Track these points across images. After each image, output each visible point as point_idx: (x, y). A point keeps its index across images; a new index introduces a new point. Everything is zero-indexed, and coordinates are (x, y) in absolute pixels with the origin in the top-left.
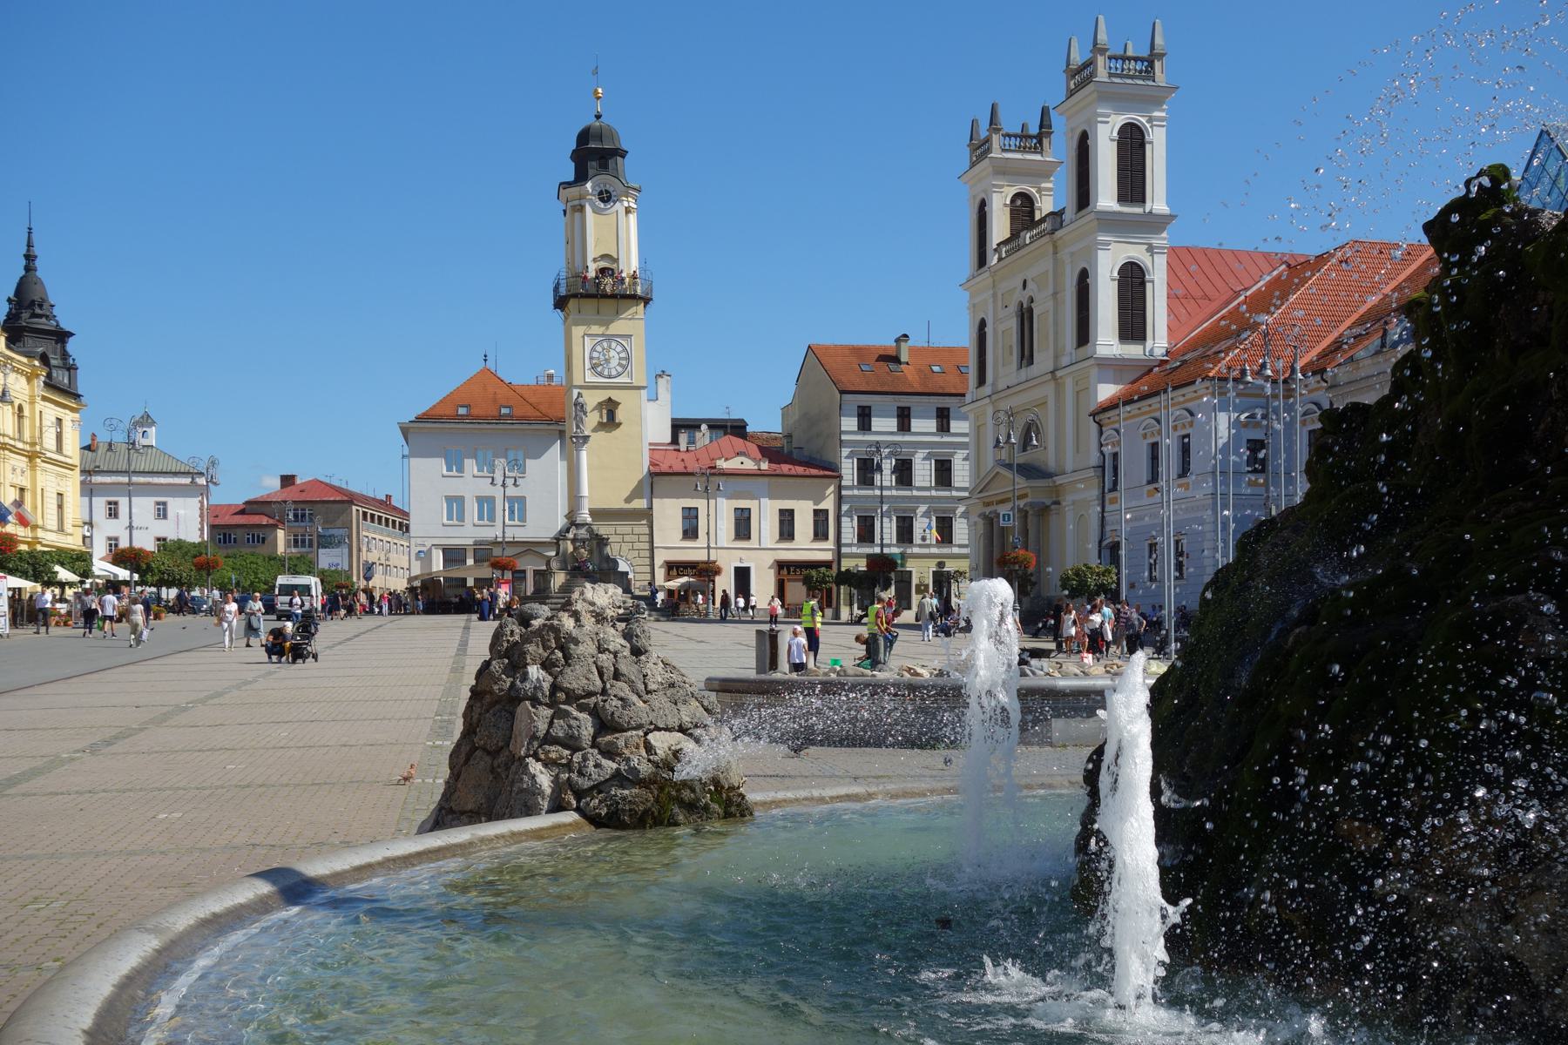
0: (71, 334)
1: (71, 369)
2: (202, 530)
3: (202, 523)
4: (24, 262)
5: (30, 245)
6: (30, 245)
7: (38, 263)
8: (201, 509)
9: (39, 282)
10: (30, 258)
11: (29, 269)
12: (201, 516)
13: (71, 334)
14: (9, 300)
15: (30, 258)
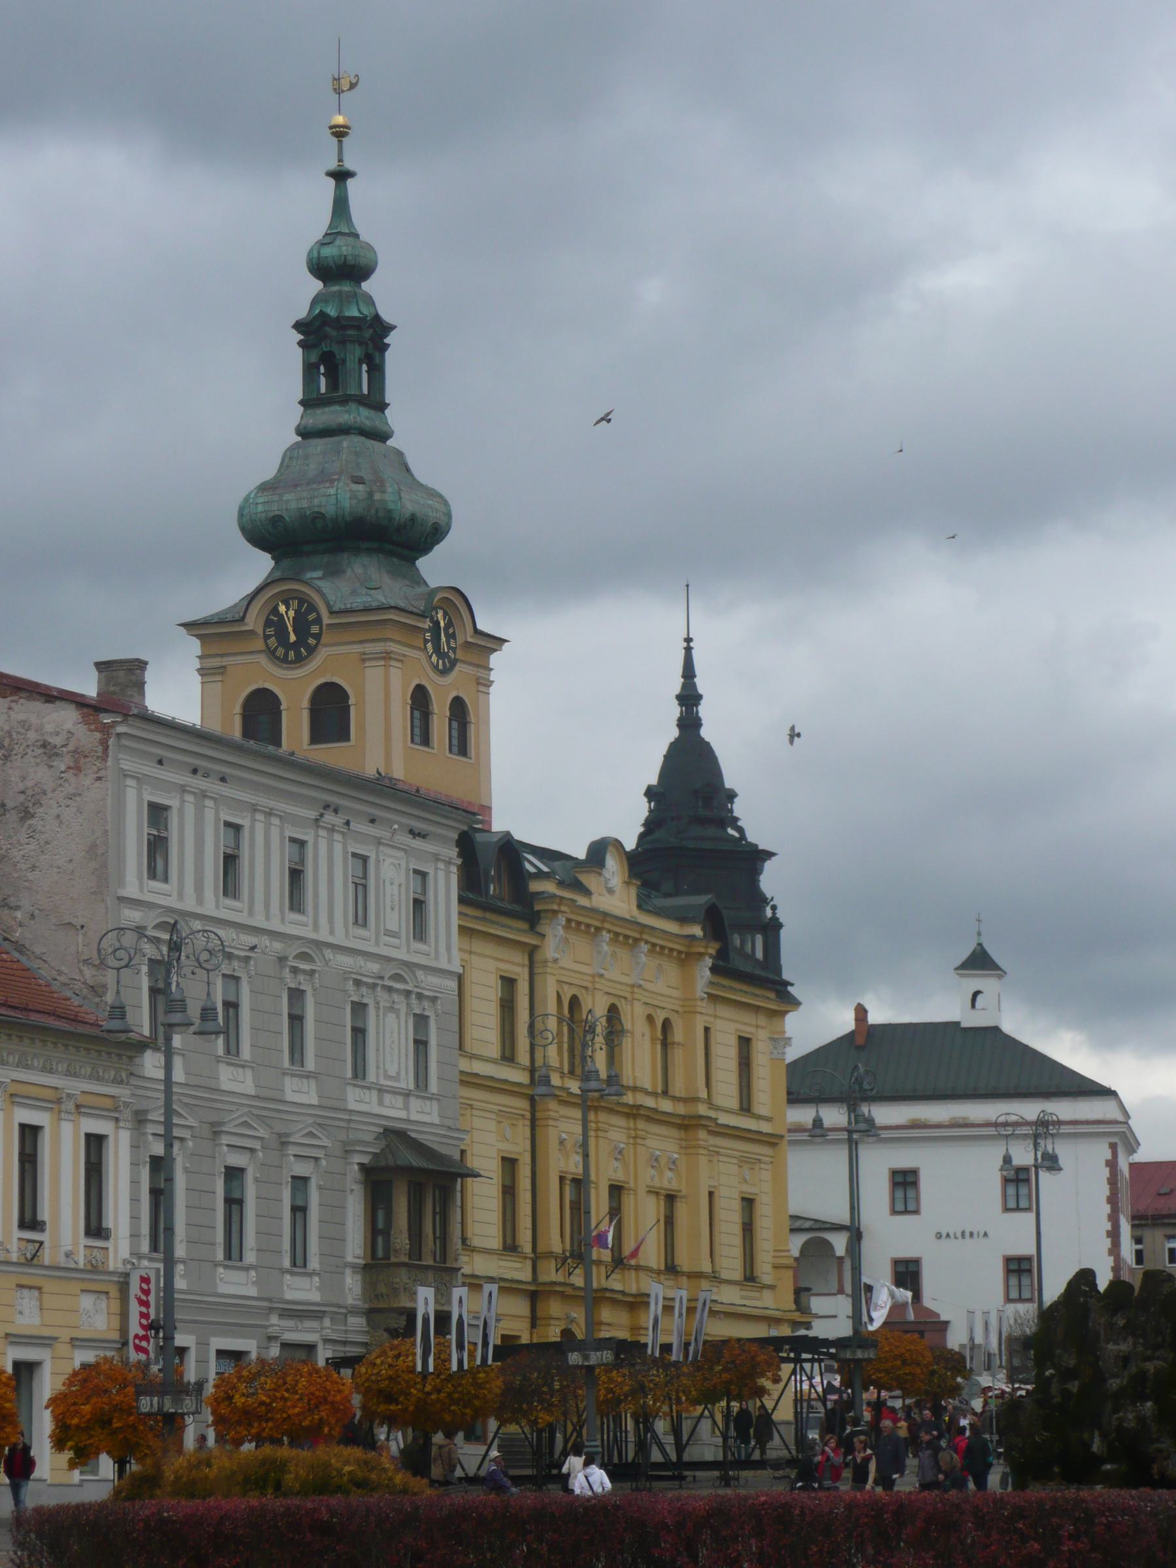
0: (770, 855)
1: (772, 928)
2: (1114, 1234)
3: (1114, 1218)
4: (675, 711)
5: (689, 672)
6: (689, 672)
7: (704, 710)
8: (1113, 1181)
9: (705, 754)
10: (689, 698)
11: (689, 723)
12: (1113, 1200)
13: (770, 855)
14: (650, 793)
15: (689, 698)
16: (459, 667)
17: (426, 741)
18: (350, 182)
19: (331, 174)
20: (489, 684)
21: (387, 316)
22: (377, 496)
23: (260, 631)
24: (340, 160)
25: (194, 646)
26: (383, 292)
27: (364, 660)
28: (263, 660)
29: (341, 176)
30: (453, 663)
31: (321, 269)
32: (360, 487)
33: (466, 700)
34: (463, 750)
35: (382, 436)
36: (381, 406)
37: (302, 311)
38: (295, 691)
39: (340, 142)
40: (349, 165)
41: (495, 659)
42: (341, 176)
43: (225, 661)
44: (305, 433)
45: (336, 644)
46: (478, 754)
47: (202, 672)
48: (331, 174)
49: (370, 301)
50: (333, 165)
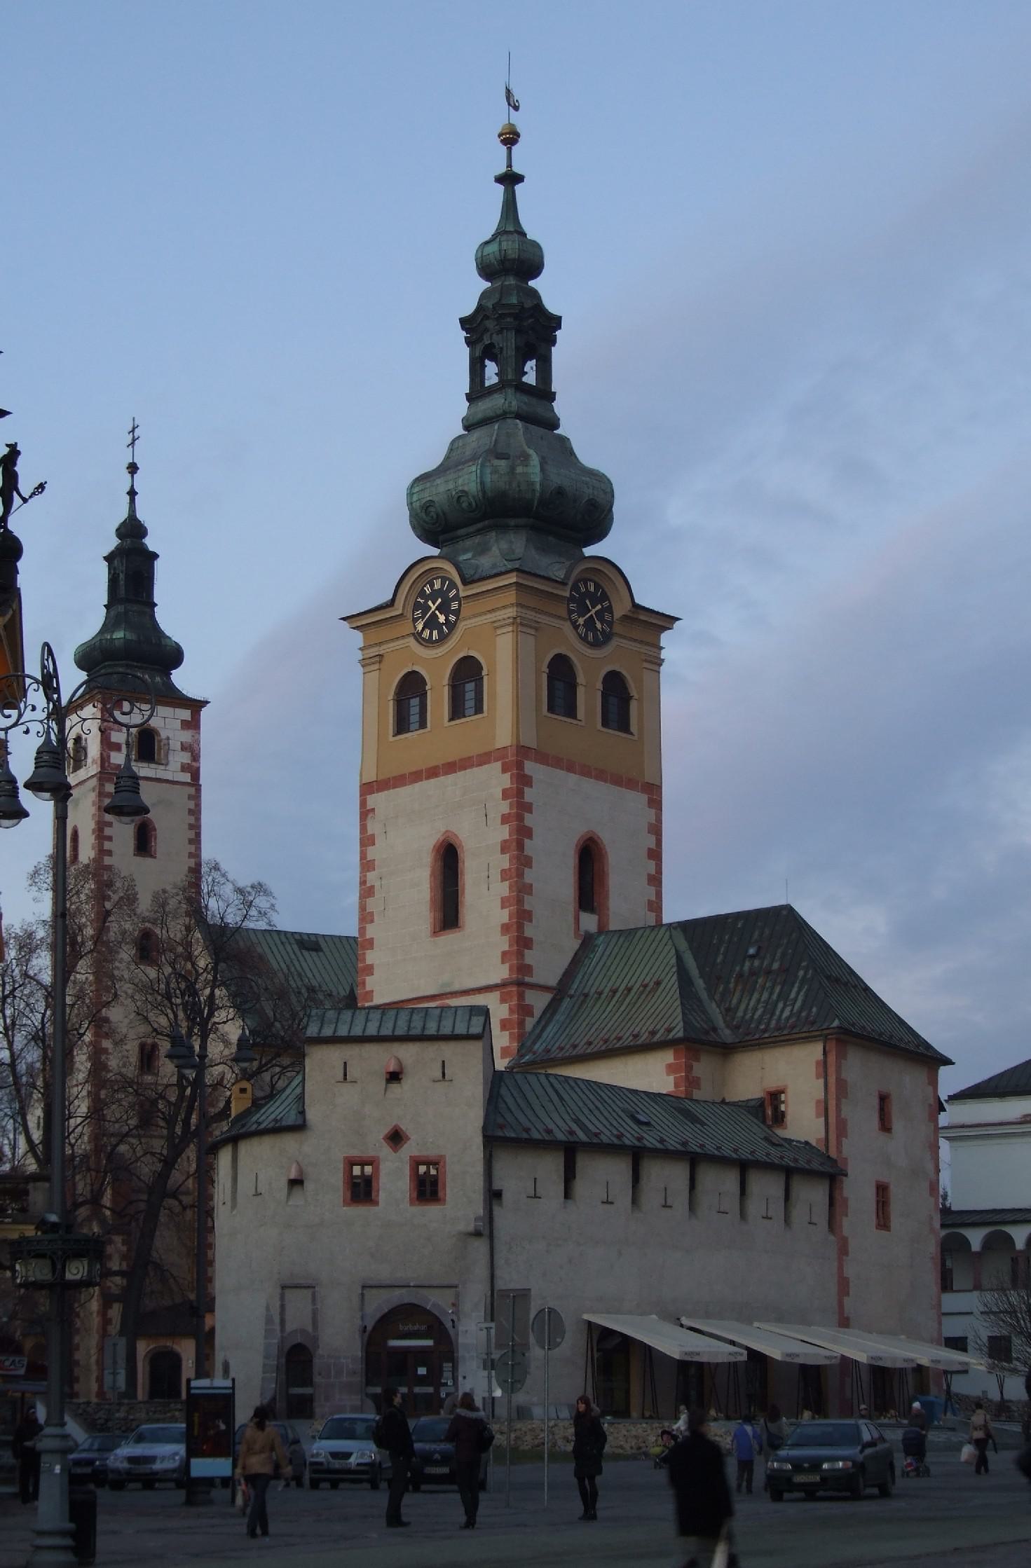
16: (615, 642)
17: (571, 712)
18: (519, 188)
19: (500, 179)
20: (660, 662)
21: (552, 305)
22: (519, 470)
23: (409, 615)
24: (509, 165)
25: (358, 638)
26: (550, 289)
27: (496, 628)
28: (411, 641)
29: (510, 180)
30: (607, 637)
31: (486, 270)
32: (503, 463)
33: (624, 673)
34: (624, 726)
35: (553, 424)
36: (551, 397)
37: (469, 308)
38: (436, 668)
39: (510, 150)
40: (517, 169)
41: (665, 638)
42: (510, 180)
43: (382, 650)
44: (469, 426)
45: (475, 616)
46: (641, 729)
47: (365, 663)
48: (500, 179)
49: (534, 294)
50: (502, 169)
